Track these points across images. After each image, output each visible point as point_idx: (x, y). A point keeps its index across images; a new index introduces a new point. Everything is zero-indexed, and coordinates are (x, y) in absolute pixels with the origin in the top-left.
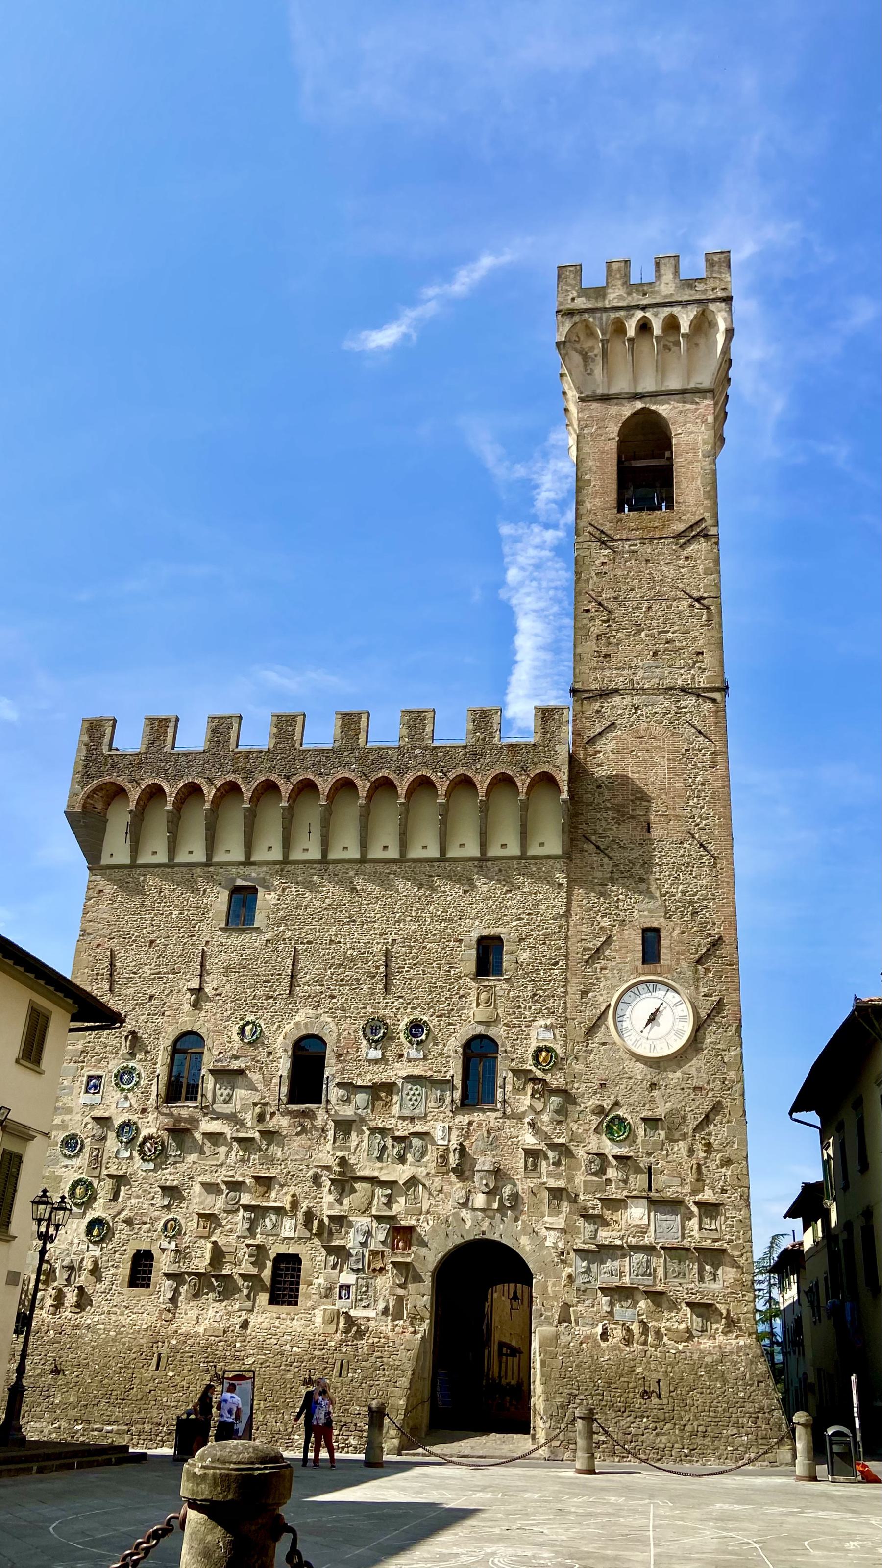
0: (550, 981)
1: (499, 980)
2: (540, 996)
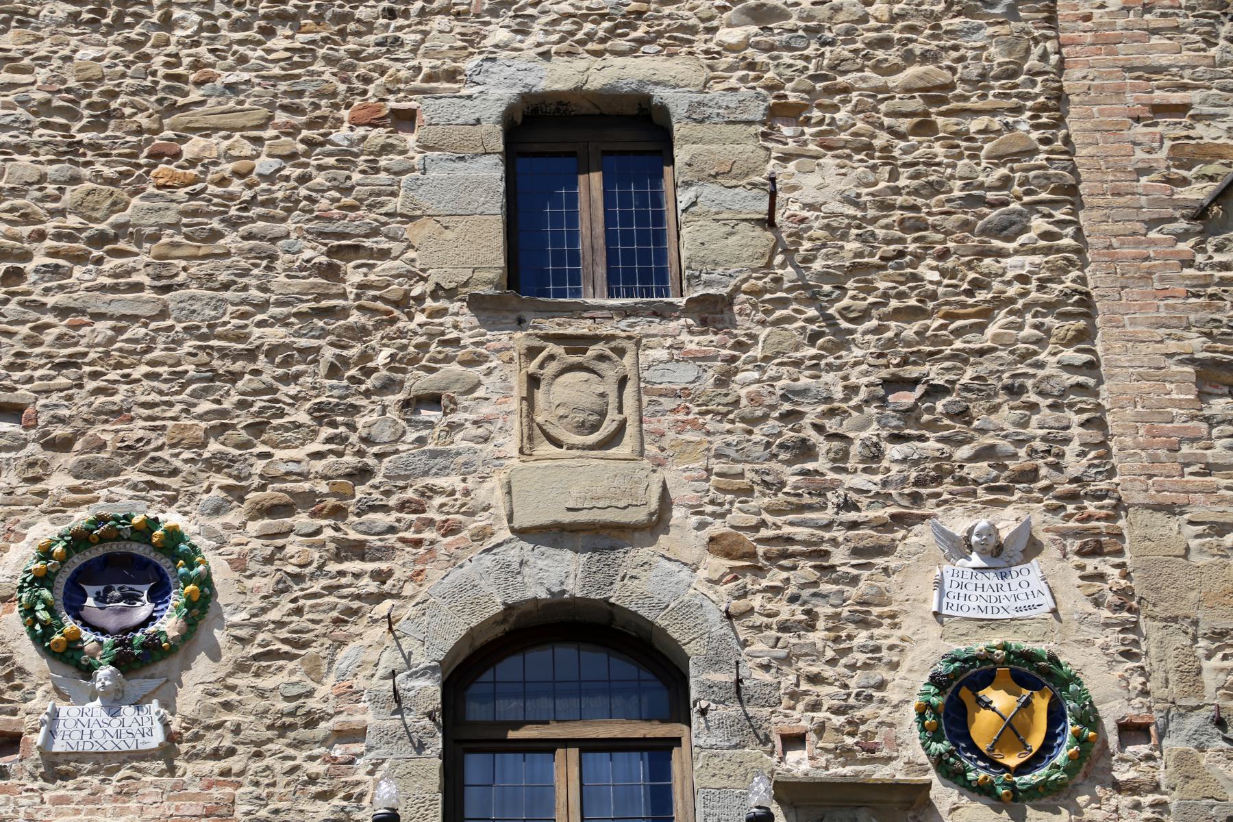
0: (987, 314)
1: (664, 313)
2: (935, 392)
